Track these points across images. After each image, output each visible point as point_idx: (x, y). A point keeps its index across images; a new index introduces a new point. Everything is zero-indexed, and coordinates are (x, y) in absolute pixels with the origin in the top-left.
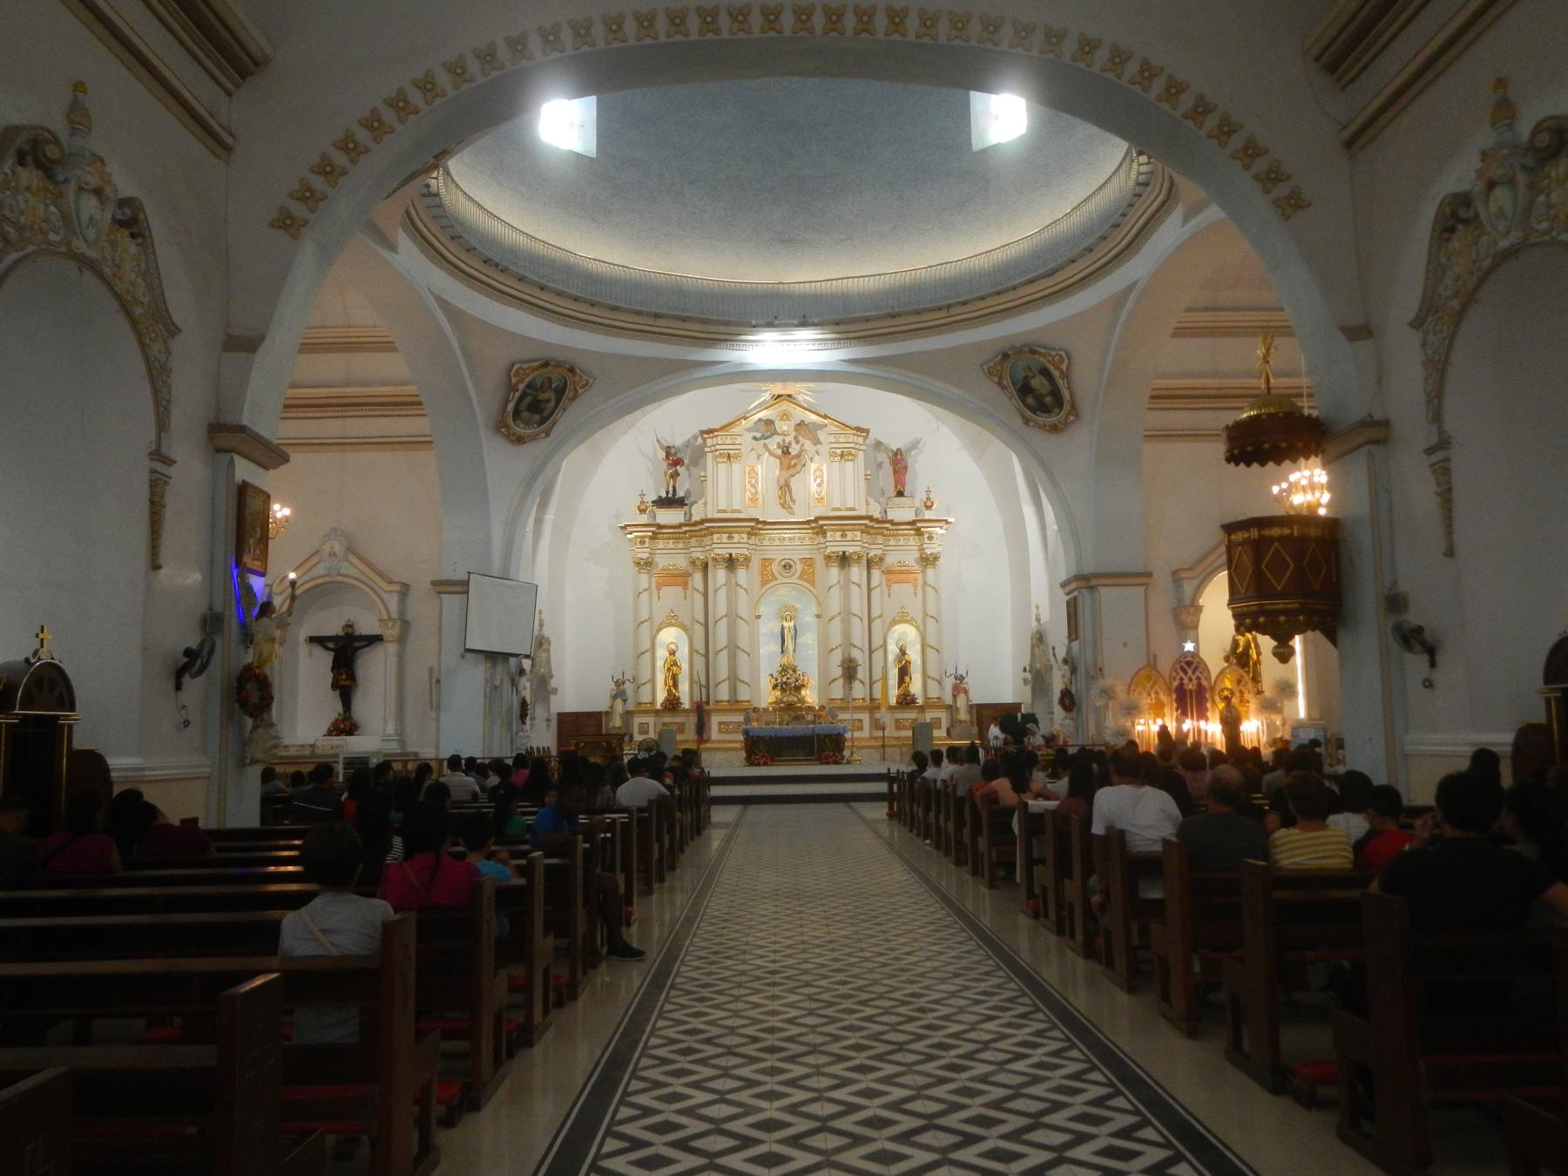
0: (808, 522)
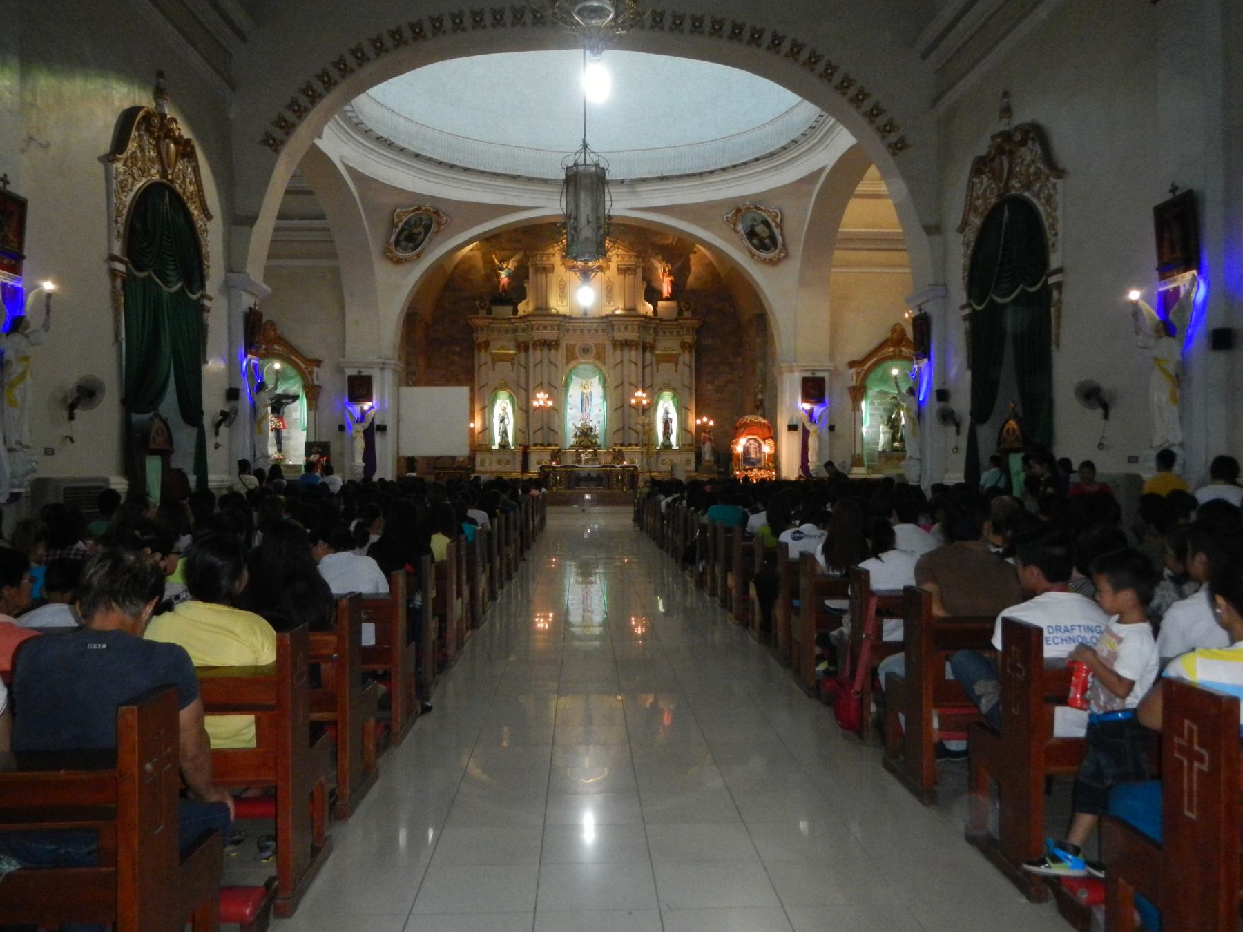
0: (602, 318)
